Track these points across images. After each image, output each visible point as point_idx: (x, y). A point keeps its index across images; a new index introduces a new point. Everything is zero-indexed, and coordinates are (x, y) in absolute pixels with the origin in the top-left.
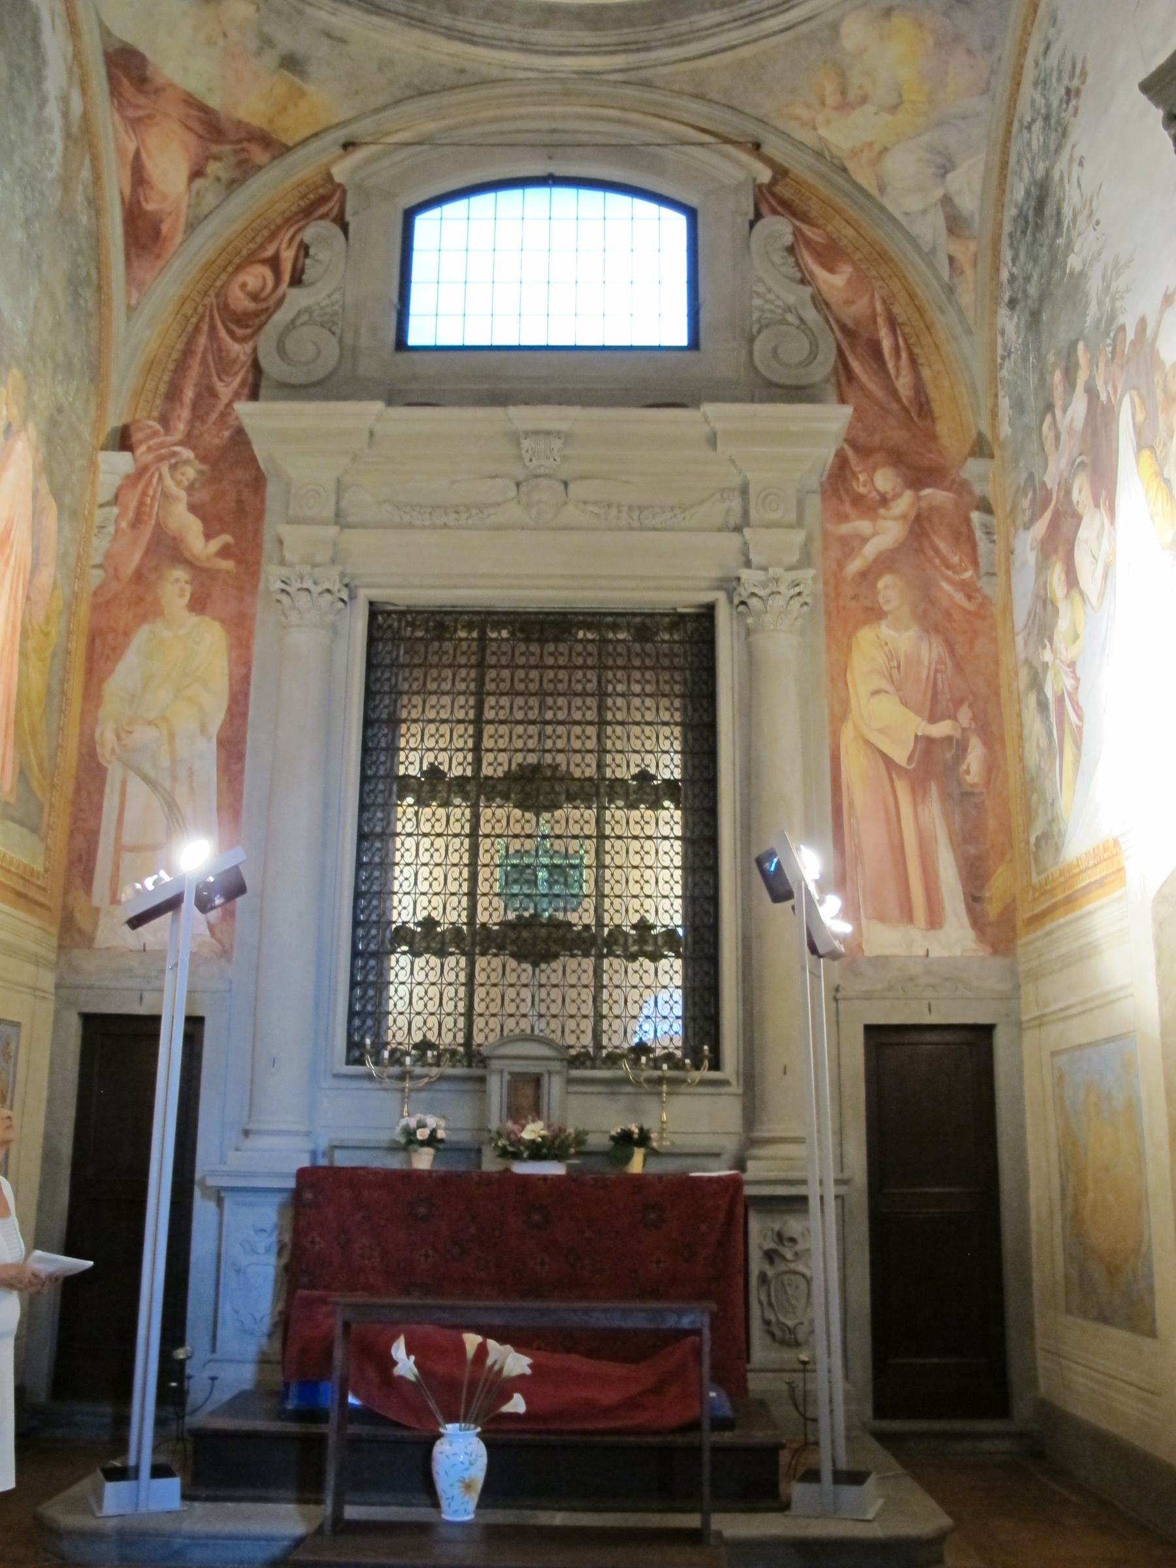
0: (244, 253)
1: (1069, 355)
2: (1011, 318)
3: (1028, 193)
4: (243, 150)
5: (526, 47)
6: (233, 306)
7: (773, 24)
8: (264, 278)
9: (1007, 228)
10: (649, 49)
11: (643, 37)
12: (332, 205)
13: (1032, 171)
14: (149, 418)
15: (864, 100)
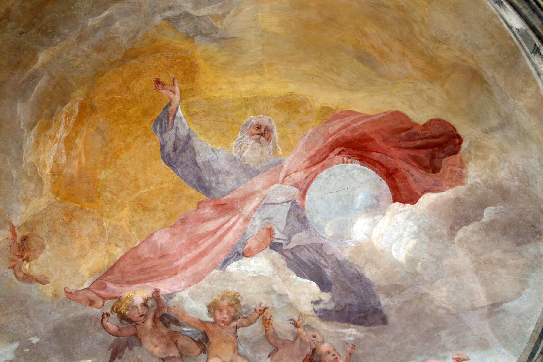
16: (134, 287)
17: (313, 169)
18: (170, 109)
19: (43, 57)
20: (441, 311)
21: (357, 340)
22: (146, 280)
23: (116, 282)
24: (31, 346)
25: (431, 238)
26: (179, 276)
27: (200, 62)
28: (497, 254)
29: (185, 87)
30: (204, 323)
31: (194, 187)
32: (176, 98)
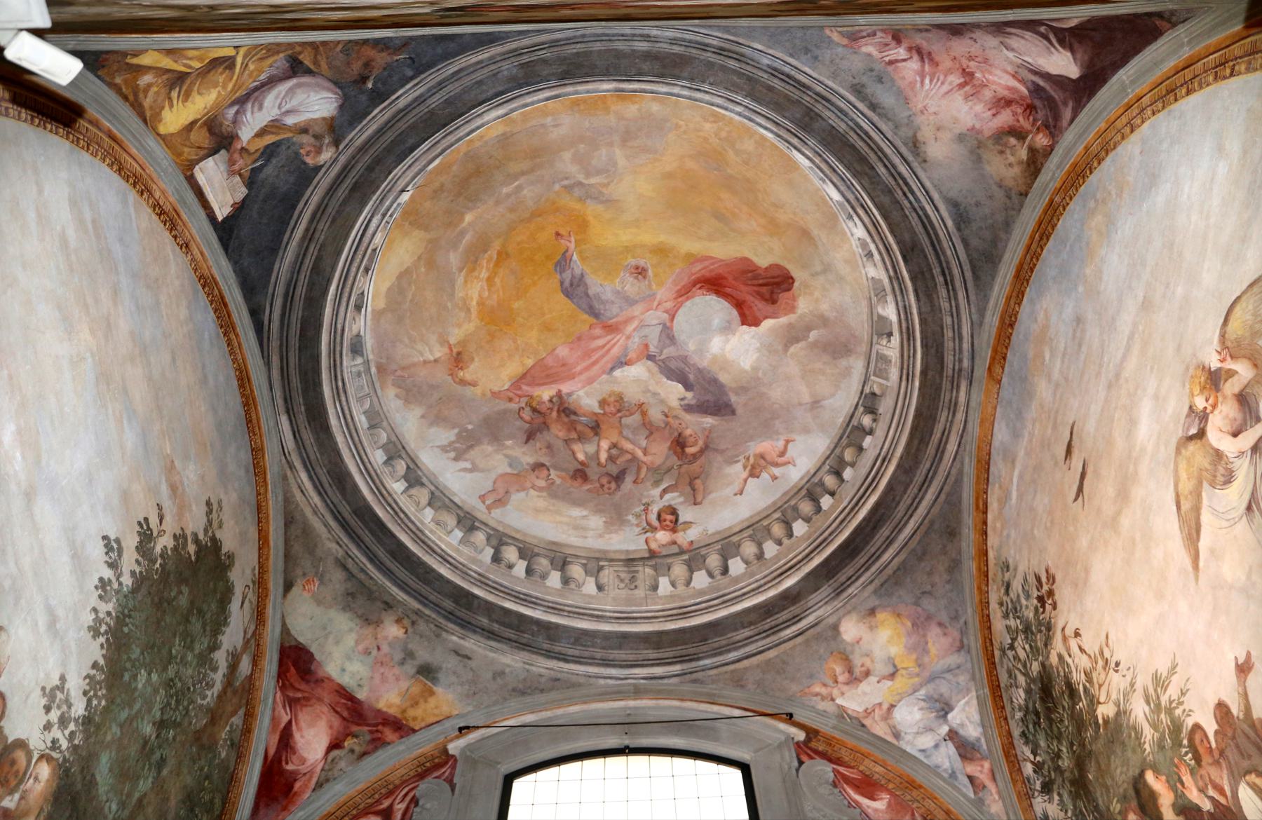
1: (1137, 792)
2: (1050, 801)
3: (1028, 691)
5: (607, 663)
7: (788, 632)
9: (1016, 733)
10: (699, 659)
11: (692, 651)
13: (1026, 675)
15: (867, 674)
16: (542, 388)
17: (680, 300)
18: (567, 254)
19: (468, 218)
20: (776, 406)
21: (713, 427)
22: (551, 383)
23: (529, 385)
24: (467, 430)
25: (770, 352)
26: (576, 379)
27: (590, 218)
28: (818, 365)
29: (578, 237)
30: (595, 414)
31: (587, 313)
32: (572, 246)
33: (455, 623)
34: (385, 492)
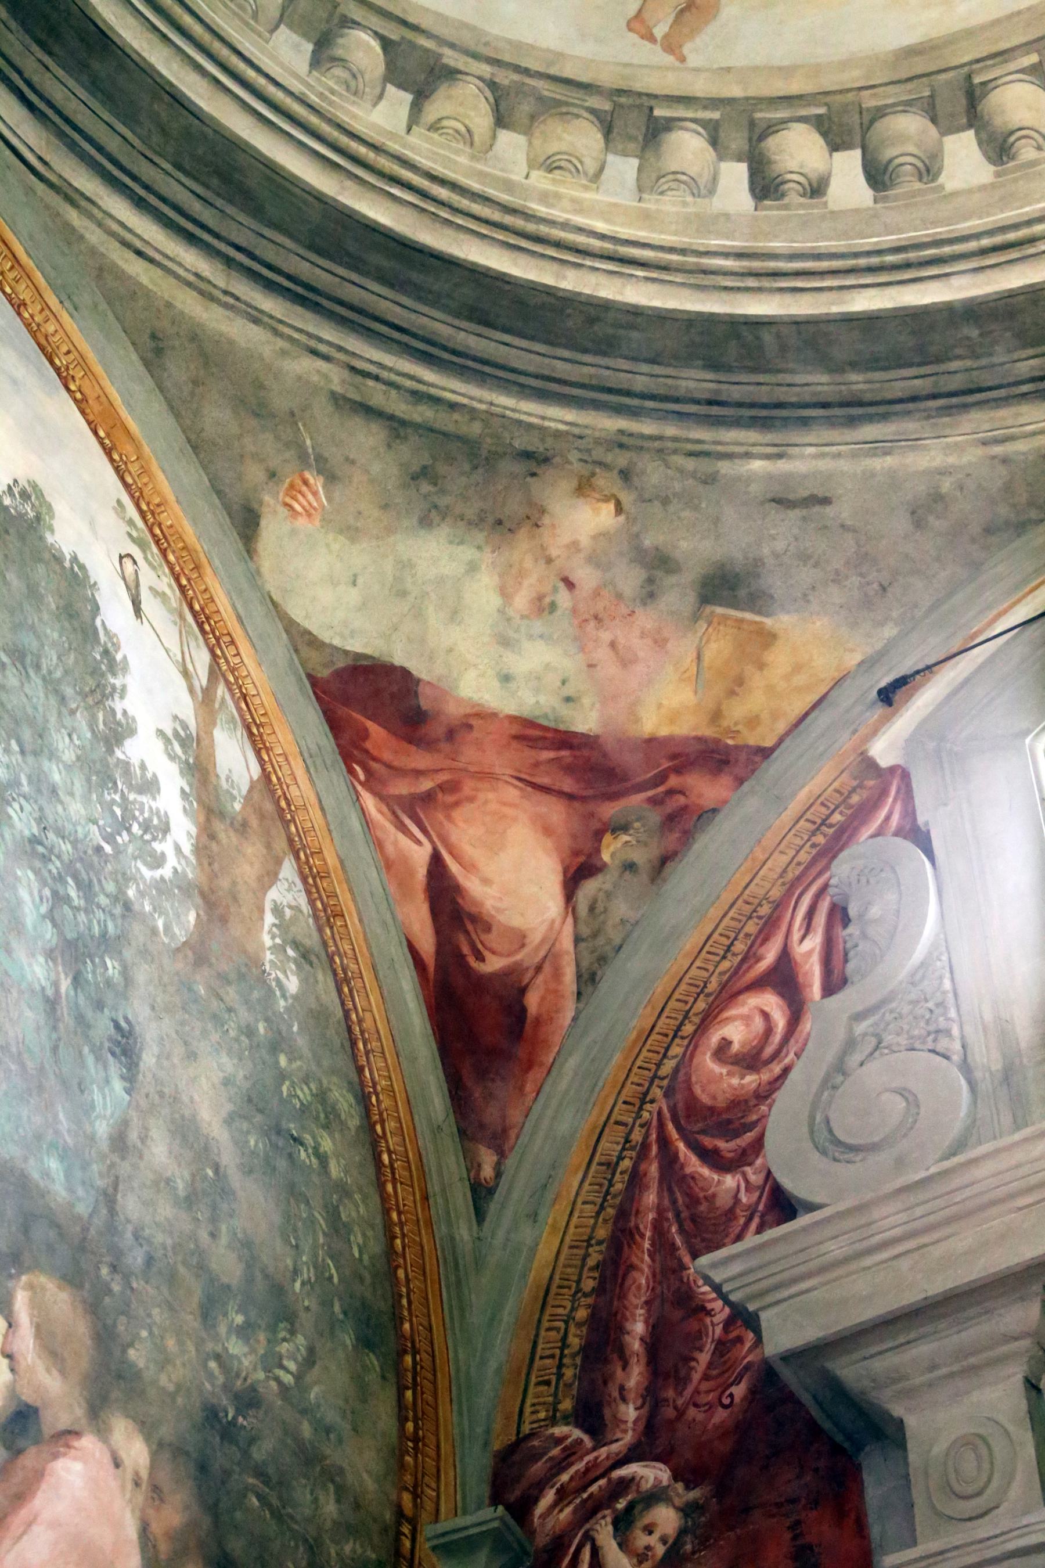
0: (713, 985)
4: (671, 792)
6: (705, 1099)
8: (766, 1016)
12: (890, 810)
14: (553, 1421)
33: (737, 423)
34: (362, 150)
